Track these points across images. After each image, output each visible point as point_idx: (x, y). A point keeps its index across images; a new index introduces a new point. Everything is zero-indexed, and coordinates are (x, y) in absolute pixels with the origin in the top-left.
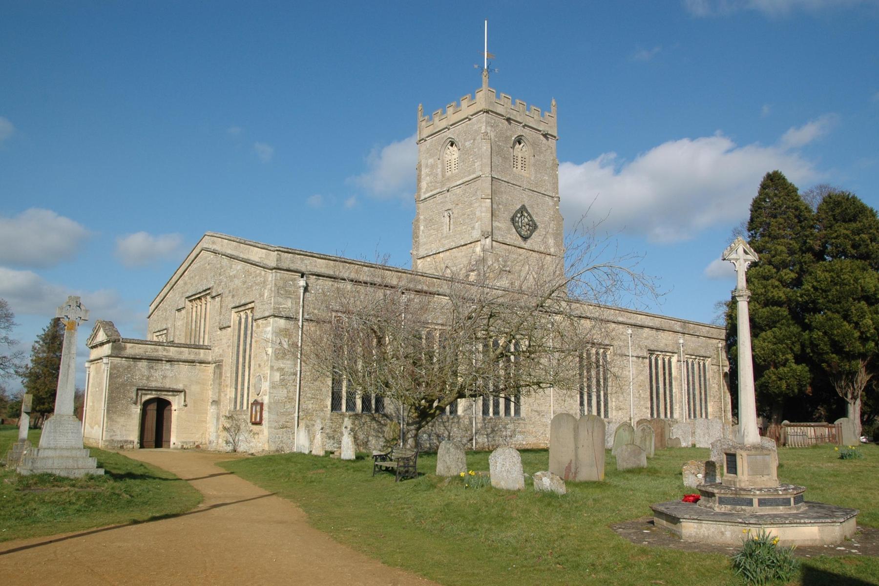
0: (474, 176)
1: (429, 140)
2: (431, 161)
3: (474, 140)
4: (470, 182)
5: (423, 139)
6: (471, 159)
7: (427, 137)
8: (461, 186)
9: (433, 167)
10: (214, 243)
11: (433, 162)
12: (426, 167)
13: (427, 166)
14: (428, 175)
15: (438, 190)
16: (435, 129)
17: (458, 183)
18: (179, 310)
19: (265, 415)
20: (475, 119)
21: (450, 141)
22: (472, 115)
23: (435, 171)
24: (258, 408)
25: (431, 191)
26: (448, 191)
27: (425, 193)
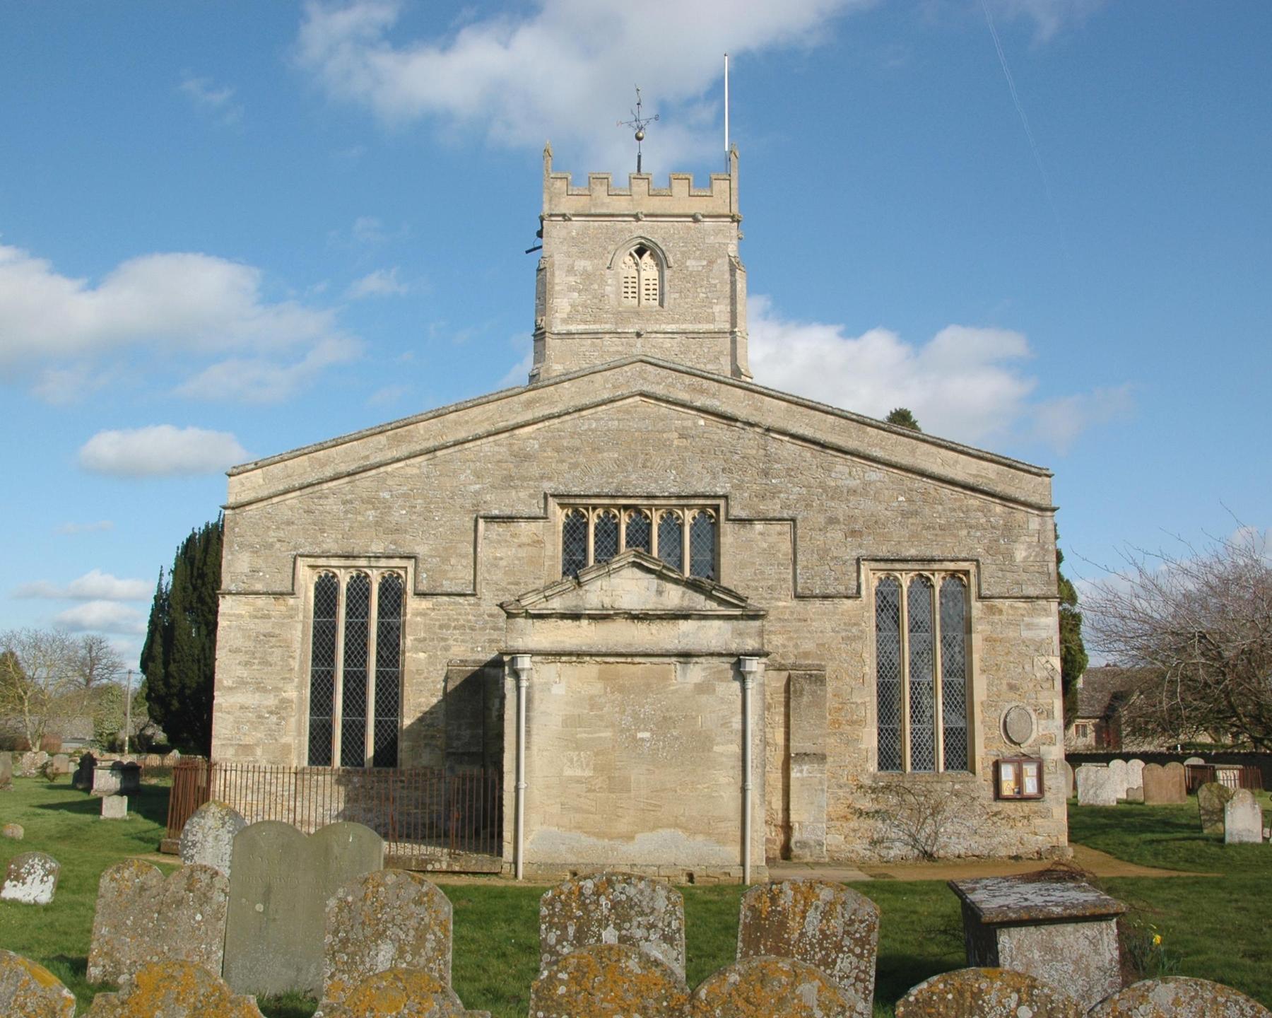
0: (711, 327)
1: (577, 223)
2: (582, 264)
3: (711, 262)
4: (701, 336)
5: (564, 215)
6: (702, 295)
7: (574, 215)
8: (675, 336)
9: (587, 276)
10: (702, 391)
11: (590, 268)
12: (568, 271)
13: (571, 270)
14: (571, 289)
15: (608, 327)
16: (595, 206)
17: (669, 328)
18: (490, 519)
19: (1048, 782)
20: (708, 224)
21: (640, 244)
22: (704, 216)
23: (596, 286)
24: (1030, 770)
25: (585, 322)
26: (639, 335)
27: (564, 321)
